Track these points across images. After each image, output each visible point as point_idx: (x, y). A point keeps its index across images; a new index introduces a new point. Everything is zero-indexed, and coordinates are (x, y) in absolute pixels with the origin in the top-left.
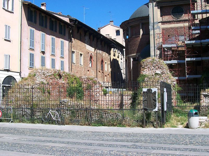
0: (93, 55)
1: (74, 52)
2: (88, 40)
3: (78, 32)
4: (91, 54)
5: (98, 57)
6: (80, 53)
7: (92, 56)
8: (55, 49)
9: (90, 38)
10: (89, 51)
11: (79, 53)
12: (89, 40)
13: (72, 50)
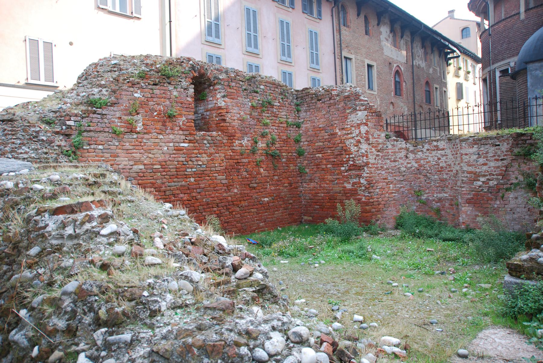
0: (402, 69)
1: (350, 59)
2: (389, 36)
3: (358, 15)
4: (398, 66)
5: (415, 75)
6: (367, 62)
7: (400, 71)
8: (292, 48)
9: (392, 31)
10: (391, 61)
12: (391, 36)
13: (344, 54)
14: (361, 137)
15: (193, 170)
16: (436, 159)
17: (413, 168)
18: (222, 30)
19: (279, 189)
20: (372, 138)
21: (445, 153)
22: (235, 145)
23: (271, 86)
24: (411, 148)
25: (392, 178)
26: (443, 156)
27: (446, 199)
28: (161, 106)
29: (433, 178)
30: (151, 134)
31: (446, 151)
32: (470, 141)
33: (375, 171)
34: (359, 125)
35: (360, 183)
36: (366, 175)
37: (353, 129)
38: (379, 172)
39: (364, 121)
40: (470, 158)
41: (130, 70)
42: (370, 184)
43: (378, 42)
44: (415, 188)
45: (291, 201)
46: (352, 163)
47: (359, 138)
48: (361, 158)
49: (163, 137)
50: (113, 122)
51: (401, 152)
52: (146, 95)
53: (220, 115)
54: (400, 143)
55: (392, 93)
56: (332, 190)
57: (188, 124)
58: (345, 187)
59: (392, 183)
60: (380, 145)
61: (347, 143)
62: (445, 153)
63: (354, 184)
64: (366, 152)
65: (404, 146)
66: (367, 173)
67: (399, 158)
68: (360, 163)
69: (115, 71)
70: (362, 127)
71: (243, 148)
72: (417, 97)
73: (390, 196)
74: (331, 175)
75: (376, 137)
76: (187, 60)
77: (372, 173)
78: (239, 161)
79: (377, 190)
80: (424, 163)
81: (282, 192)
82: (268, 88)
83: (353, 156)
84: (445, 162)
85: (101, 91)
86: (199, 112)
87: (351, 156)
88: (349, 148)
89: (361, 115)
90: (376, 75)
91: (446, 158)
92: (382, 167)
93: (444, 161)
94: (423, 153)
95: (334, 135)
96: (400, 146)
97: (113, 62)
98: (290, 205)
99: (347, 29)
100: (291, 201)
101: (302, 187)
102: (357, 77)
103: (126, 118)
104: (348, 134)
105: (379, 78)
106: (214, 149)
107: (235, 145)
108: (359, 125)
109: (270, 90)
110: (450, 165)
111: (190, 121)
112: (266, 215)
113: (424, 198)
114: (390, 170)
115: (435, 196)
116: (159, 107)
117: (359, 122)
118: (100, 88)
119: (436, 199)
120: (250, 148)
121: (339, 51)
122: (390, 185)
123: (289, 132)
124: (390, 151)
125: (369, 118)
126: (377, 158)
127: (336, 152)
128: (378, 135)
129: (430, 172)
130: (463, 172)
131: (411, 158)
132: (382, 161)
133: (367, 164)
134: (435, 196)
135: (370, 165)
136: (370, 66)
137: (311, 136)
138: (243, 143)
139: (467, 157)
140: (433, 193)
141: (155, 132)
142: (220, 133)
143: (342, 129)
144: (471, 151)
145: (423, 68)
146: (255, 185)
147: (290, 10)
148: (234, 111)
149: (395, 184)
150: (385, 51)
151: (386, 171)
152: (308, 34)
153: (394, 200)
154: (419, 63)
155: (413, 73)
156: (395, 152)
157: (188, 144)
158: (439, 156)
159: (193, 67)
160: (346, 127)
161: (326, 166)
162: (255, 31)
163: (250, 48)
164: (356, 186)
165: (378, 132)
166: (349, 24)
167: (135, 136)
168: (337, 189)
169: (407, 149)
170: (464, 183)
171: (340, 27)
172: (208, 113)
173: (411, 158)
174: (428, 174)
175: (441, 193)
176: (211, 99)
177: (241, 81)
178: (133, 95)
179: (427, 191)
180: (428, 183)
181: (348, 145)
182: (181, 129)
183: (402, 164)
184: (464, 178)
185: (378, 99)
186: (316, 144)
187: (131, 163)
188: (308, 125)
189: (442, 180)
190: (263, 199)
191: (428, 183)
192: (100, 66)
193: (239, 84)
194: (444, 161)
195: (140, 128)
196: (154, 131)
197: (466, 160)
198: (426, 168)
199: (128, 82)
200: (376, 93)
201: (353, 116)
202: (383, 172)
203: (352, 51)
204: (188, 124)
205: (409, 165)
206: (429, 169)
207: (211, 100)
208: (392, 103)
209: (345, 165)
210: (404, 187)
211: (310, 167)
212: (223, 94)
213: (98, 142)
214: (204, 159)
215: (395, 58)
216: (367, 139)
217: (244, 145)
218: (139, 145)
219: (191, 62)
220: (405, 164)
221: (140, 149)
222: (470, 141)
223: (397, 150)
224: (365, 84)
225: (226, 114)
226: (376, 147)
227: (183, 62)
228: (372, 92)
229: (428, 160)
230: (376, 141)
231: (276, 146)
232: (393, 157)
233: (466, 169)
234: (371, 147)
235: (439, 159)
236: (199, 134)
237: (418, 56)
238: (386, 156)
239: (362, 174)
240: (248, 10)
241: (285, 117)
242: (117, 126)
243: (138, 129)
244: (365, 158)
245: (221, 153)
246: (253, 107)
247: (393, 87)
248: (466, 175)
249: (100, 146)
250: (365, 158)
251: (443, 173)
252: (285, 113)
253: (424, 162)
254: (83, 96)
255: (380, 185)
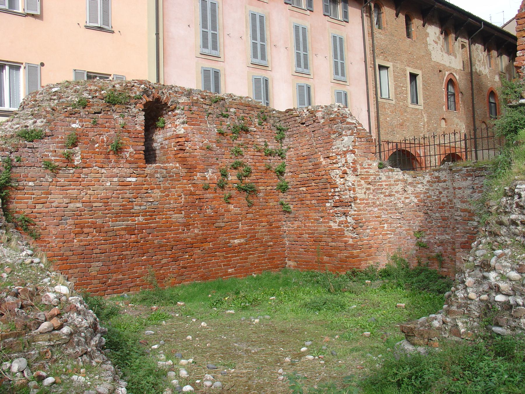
0: (457, 77)
1: (387, 68)
2: (439, 38)
5: (474, 84)
6: (409, 70)
7: (454, 80)
8: (310, 57)
10: (441, 68)
11: (404, 71)
13: (378, 62)
14: (348, 167)
15: (142, 207)
16: (437, 193)
17: (412, 204)
18: (220, 40)
19: (254, 229)
20: (361, 169)
21: (447, 185)
22: (195, 178)
23: (246, 108)
24: (410, 180)
25: (386, 216)
26: (444, 189)
27: (448, 242)
28: (104, 137)
29: (434, 216)
30: (91, 169)
31: (447, 183)
32: (463, 172)
33: (364, 207)
34: (345, 153)
35: (346, 222)
36: (353, 212)
37: (339, 157)
38: (370, 209)
39: (351, 148)
40: (464, 192)
41: (70, 98)
42: (359, 224)
43: (423, 46)
44: (414, 228)
45: (271, 243)
46: (337, 198)
47: (346, 168)
48: (348, 192)
49: (105, 172)
50: (46, 156)
51: (397, 185)
52: (86, 125)
53: (178, 144)
54: (396, 173)
55: (444, 107)
56: (317, 230)
57: (136, 156)
58: (330, 227)
59: (387, 221)
60: (371, 177)
61: (333, 174)
62: (447, 185)
63: (341, 223)
64: (353, 184)
65: (401, 177)
66: (355, 211)
67: (396, 192)
68: (346, 198)
69: (55, 100)
70: (348, 156)
71: (206, 182)
72: (478, 111)
73: (385, 237)
74: (315, 213)
75: (366, 167)
76: (138, 83)
77: (360, 210)
78: (201, 197)
79: (368, 231)
80: (425, 198)
81: (258, 232)
82: (241, 111)
83: (339, 189)
84: (447, 197)
85: (35, 122)
86: (158, 141)
87: (337, 190)
88: (335, 180)
89: (347, 140)
90: (421, 86)
91: (448, 192)
92: (374, 203)
93: (445, 195)
94: (423, 186)
95: (317, 165)
96: (397, 177)
97: (54, 90)
98: (269, 247)
99: (383, 32)
100: (271, 243)
101: (286, 227)
102: (395, 89)
103: (62, 151)
104: (334, 163)
105: (425, 89)
106: (169, 184)
107: (195, 178)
108: (345, 153)
109: (244, 113)
110: (451, 201)
111: (139, 152)
112: (237, 260)
113: (425, 240)
114: (384, 207)
115: (437, 238)
116: (101, 138)
117: (345, 149)
118: (35, 120)
119: (438, 242)
120: (216, 181)
121: (372, 58)
122: (384, 224)
123: (269, 161)
124: (384, 183)
125: (357, 144)
126: (367, 192)
127: (321, 185)
128: (368, 165)
129: (431, 208)
130: (456, 209)
131: (410, 192)
132: (374, 196)
133: (355, 199)
134: (437, 238)
135: (358, 201)
136: (413, 77)
137: (294, 166)
138: (207, 176)
139: (461, 191)
140: (435, 235)
141: (96, 166)
142: (178, 165)
143: (328, 157)
144: (465, 184)
145: (486, 75)
146: (223, 225)
147: (308, 12)
148: (196, 140)
149: (391, 223)
150: (433, 56)
151: (379, 208)
152: (331, 40)
153: (389, 242)
154: (481, 69)
155: (472, 82)
156: (390, 185)
157: (136, 179)
158: (441, 190)
159: (145, 92)
160: (331, 155)
161: (310, 202)
162: (263, 39)
163: (256, 59)
164: (342, 225)
165: (369, 161)
166: (385, 26)
167: (72, 171)
168: (322, 229)
169: (405, 181)
170: (458, 223)
171: (372, 30)
172: (167, 142)
173: (410, 192)
174: (429, 212)
175: (443, 235)
176: (170, 126)
177: (205, 104)
178: (70, 125)
179: (428, 232)
180: (429, 222)
181: (334, 177)
182: (127, 161)
183: (399, 199)
184: (457, 218)
185: (424, 115)
186: (300, 176)
187: (66, 200)
188: (292, 153)
189: (444, 219)
190: (232, 241)
191: (429, 222)
192: (40, 94)
193: (202, 107)
194: (445, 195)
195: (78, 162)
196: (94, 165)
197: (460, 196)
198: (426, 204)
199: (66, 111)
200: (422, 108)
201: (338, 142)
202: (376, 209)
203: (389, 58)
204: (136, 156)
205: (407, 201)
206: (430, 205)
207: (170, 128)
208: (444, 119)
209: (330, 201)
210: (401, 227)
211: (294, 203)
212: (181, 120)
213: (29, 178)
214: (156, 195)
215: (447, 64)
216: (355, 170)
217: (208, 178)
218: (77, 181)
219: (143, 86)
220: (403, 199)
221: (77, 185)
222: (463, 172)
223: (392, 182)
224: (407, 97)
225: (186, 143)
226: (366, 178)
227: (133, 86)
228: (417, 107)
229: (428, 195)
230: (366, 172)
231: (251, 178)
232: (388, 191)
233: (459, 207)
234: (359, 179)
235: (440, 193)
236: (150, 167)
237: (479, 61)
238: (378, 189)
239: (350, 211)
240: (253, 16)
241: (263, 144)
242: (51, 160)
243: (76, 163)
244: (352, 192)
245: (179, 188)
246: (221, 134)
247: (445, 100)
248: (459, 213)
249: (30, 183)
250: (352, 192)
251: (444, 211)
252: (263, 139)
253: (424, 196)
254: (16, 129)
255: (372, 225)
